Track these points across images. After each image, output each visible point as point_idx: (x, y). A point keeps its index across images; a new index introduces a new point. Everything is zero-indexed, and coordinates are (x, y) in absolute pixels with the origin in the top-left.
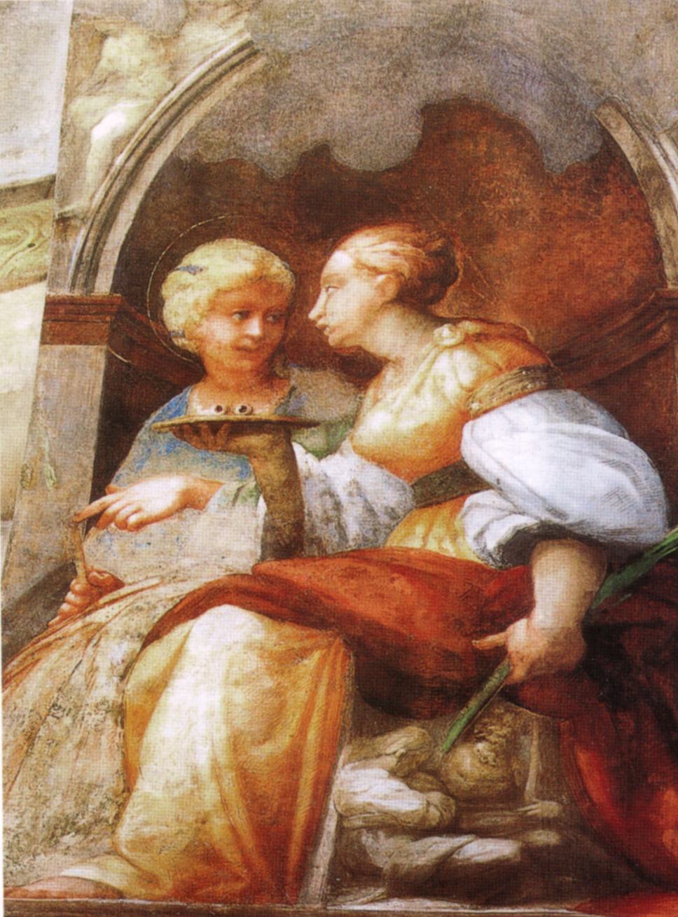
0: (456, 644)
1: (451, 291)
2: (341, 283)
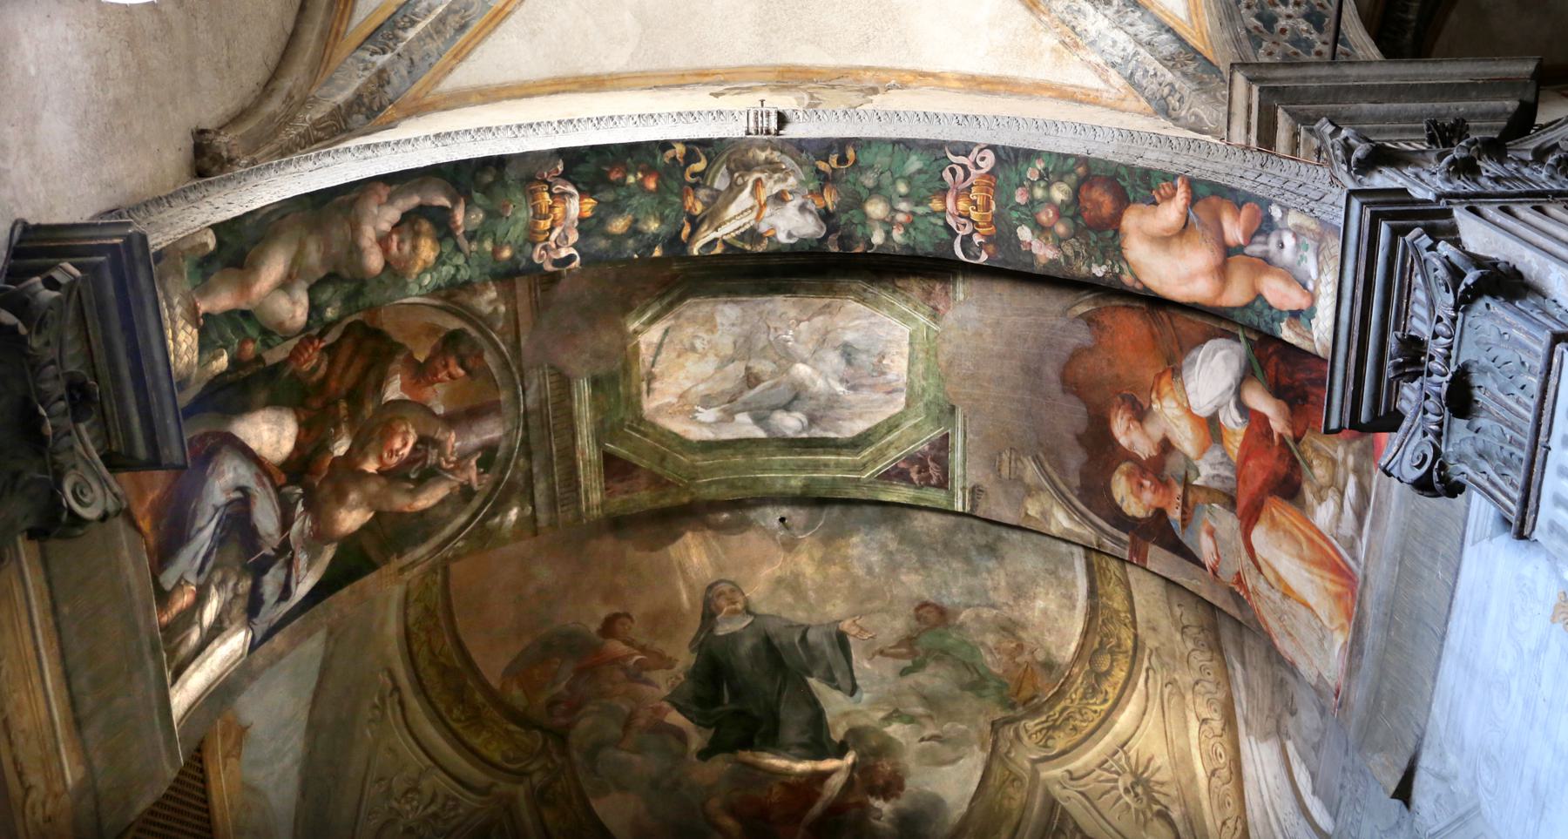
0: (1275, 453)
1: (1139, 399)
2: (1132, 444)
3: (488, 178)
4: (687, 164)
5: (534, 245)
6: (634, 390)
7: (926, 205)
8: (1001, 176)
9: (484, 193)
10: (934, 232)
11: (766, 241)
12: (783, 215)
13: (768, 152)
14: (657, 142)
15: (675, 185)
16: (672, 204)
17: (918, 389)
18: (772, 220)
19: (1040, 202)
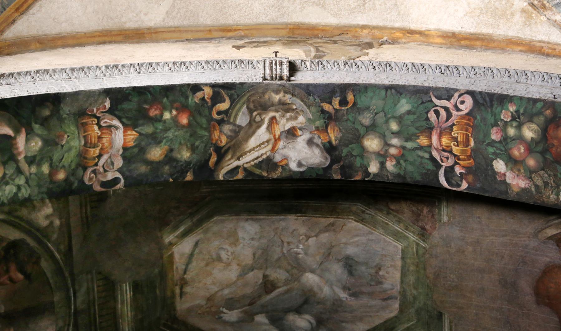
3: (46, 112)
4: (214, 103)
5: (85, 169)
6: (169, 293)
7: (414, 141)
8: (478, 117)
9: (42, 124)
10: (421, 163)
11: (280, 169)
12: (294, 148)
13: (281, 95)
14: (188, 85)
15: (204, 121)
16: (202, 137)
17: (410, 298)
18: (286, 152)
19: (513, 139)
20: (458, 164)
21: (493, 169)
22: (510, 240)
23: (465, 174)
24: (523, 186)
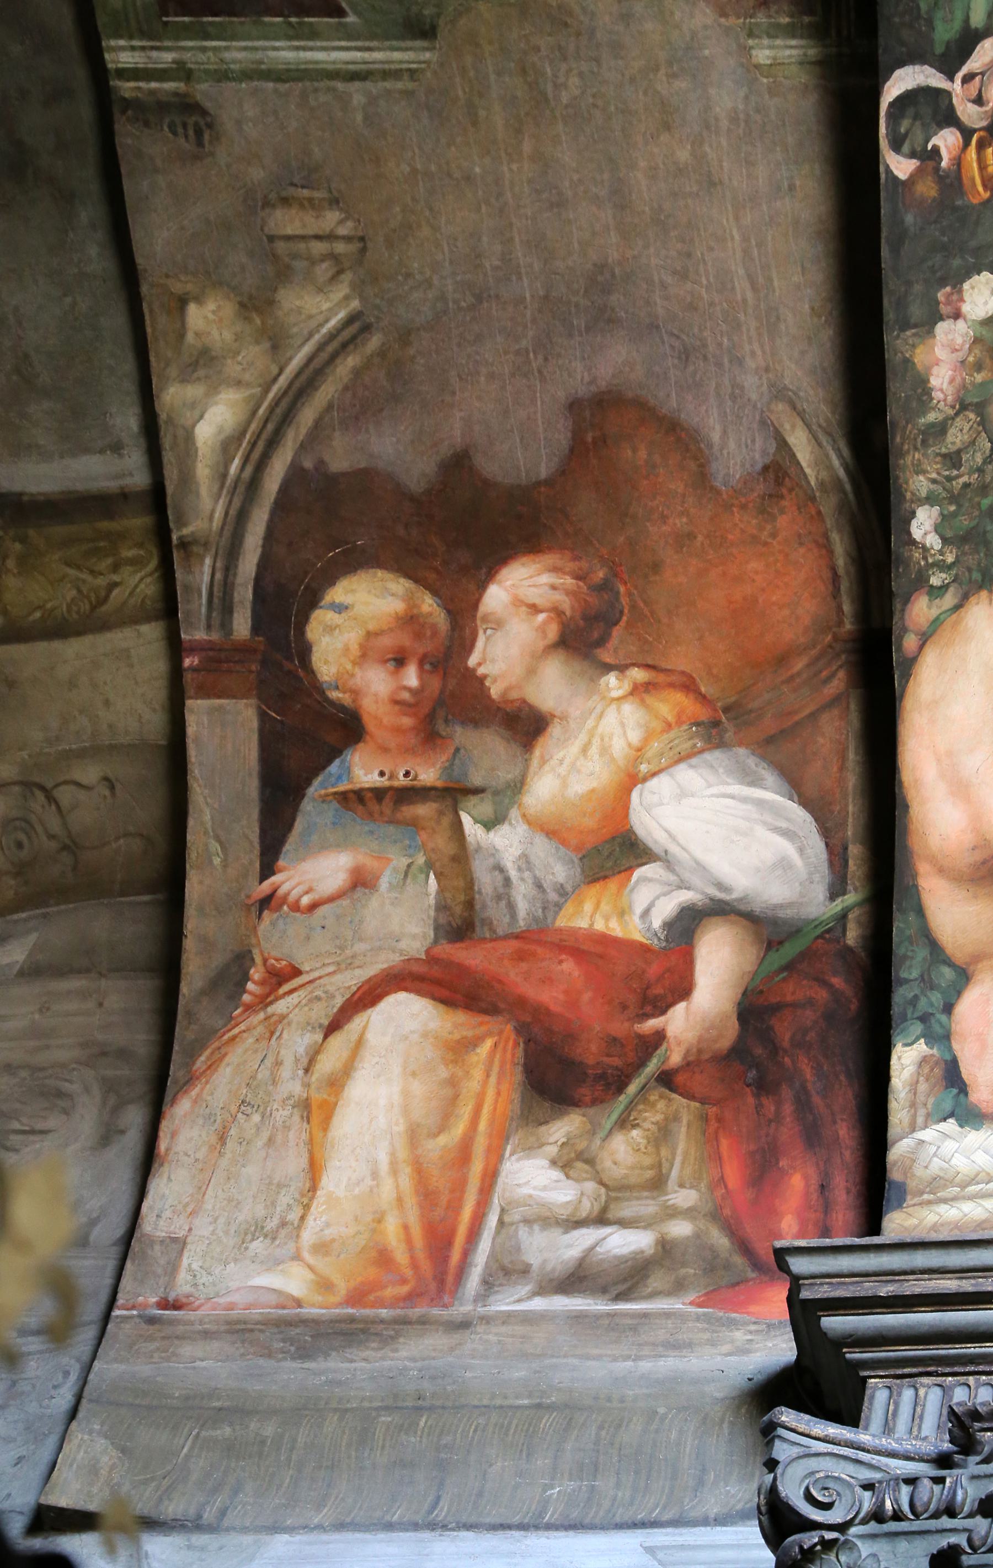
20: (967, 143)
21: (968, 276)
22: (744, 301)
23: (937, 169)
24: (934, 382)
